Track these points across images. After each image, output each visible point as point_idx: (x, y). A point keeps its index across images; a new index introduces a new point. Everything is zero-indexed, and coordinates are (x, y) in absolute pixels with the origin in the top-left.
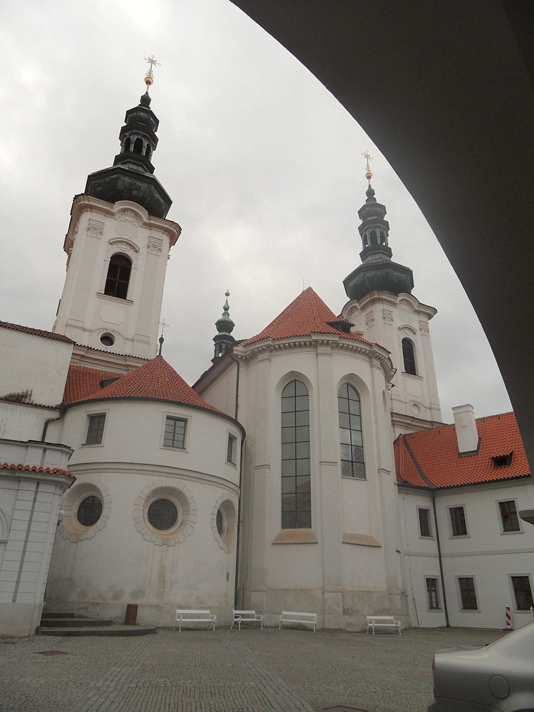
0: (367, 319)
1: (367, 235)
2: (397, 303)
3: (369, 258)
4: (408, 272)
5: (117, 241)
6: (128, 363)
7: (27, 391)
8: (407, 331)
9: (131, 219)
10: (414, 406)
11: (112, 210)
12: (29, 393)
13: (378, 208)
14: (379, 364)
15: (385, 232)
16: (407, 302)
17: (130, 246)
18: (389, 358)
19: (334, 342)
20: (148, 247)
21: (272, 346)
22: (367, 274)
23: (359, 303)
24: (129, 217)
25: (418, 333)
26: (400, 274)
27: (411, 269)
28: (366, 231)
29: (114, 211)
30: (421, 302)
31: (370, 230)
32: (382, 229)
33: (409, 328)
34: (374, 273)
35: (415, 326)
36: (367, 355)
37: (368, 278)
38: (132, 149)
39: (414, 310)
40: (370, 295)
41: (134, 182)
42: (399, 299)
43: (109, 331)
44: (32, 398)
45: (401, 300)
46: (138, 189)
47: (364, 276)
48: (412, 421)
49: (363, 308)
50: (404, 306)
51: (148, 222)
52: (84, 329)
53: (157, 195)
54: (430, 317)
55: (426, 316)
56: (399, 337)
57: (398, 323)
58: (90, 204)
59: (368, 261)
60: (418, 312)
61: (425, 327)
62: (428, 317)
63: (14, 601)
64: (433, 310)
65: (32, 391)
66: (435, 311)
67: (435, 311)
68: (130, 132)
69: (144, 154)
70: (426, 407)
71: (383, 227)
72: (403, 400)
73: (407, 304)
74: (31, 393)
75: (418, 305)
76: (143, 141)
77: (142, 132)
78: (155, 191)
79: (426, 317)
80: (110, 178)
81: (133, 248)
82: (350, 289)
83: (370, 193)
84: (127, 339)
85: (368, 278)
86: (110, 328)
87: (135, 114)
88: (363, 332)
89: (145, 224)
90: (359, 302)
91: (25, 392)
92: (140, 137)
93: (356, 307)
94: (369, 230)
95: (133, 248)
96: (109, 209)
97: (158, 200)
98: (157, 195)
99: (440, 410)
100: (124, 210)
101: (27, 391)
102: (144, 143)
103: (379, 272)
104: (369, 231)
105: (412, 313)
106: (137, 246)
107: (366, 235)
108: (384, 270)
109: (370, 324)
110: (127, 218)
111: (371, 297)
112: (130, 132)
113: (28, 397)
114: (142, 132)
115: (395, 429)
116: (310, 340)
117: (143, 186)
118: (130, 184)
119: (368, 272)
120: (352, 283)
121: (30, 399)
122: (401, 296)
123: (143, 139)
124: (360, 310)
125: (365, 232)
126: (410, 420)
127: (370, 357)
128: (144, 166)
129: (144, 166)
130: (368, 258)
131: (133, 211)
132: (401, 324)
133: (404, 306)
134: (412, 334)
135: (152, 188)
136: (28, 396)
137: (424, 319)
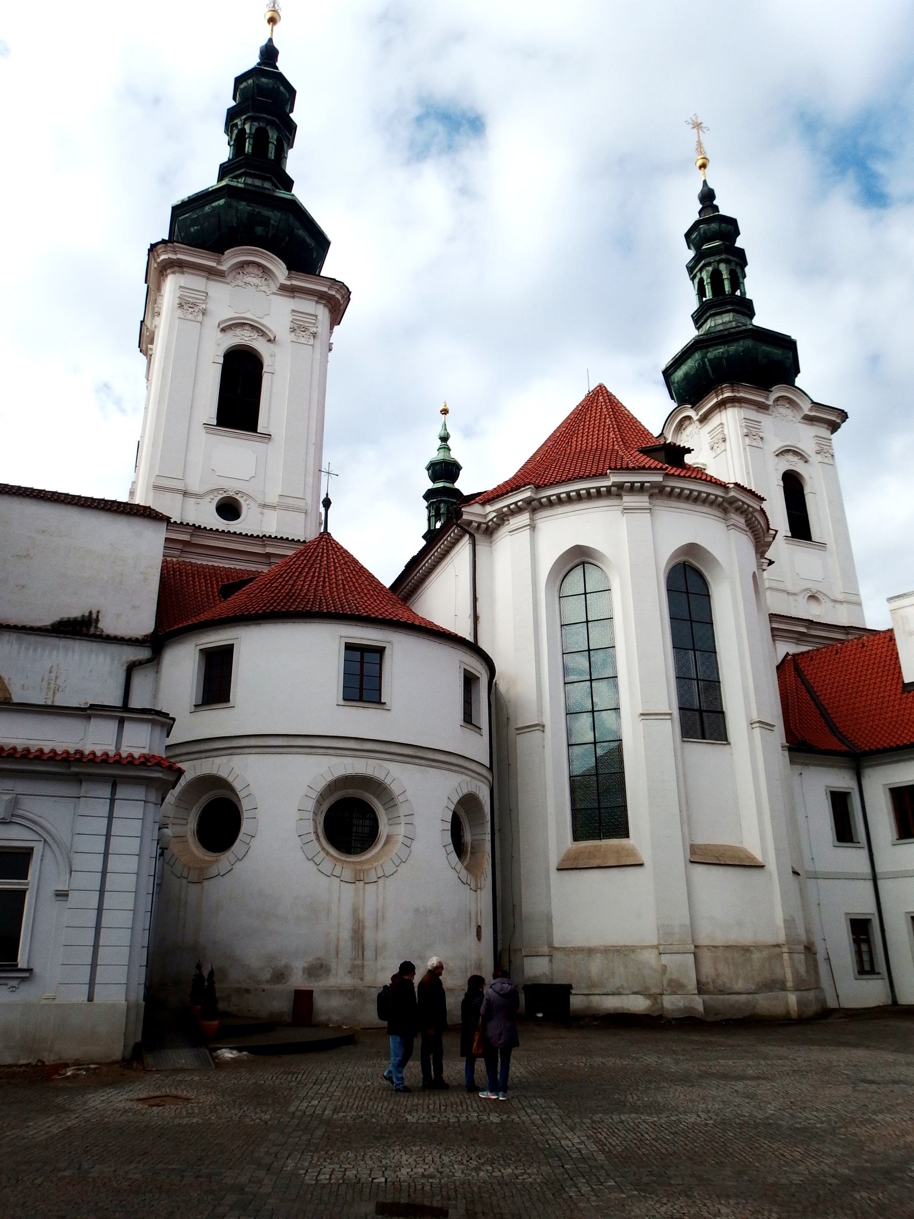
0: (712, 439)
1: (705, 278)
2: (770, 405)
3: (710, 324)
4: (788, 345)
5: (233, 325)
6: (269, 550)
7: (91, 613)
8: (790, 457)
9: (256, 281)
10: (811, 598)
12: (94, 616)
13: (723, 225)
14: (744, 522)
15: (738, 270)
16: (788, 401)
17: (258, 332)
18: (762, 509)
19: (654, 485)
20: (293, 330)
21: (534, 500)
22: (707, 352)
23: (695, 410)
24: (252, 278)
25: (814, 459)
26: (771, 350)
27: (792, 338)
28: (701, 270)
29: (224, 267)
30: (815, 401)
31: (710, 269)
32: (733, 264)
33: (794, 451)
34: (721, 350)
36: (720, 505)
37: (709, 360)
39: (802, 416)
40: (716, 392)
41: (257, 210)
42: (774, 396)
43: (231, 494)
44: (100, 625)
45: (777, 399)
46: (265, 222)
47: (703, 359)
48: (807, 628)
49: (703, 419)
50: (782, 410)
51: (288, 283)
52: (185, 494)
53: (301, 232)
54: (834, 427)
55: (826, 426)
56: (776, 470)
57: (775, 443)
59: (710, 327)
61: (825, 447)
62: (830, 428)
63: (90, 999)
64: (839, 414)
65: (98, 612)
66: (844, 415)
67: (844, 415)
68: (244, 117)
69: (272, 155)
70: (835, 601)
71: (734, 261)
72: (790, 589)
73: (787, 406)
74: (98, 616)
75: (810, 406)
76: (269, 131)
77: (265, 116)
78: (297, 224)
79: (827, 429)
82: (676, 385)
83: (707, 197)
85: (709, 360)
86: (231, 487)
87: (250, 81)
88: (705, 465)
89: (283, 288)
90: (695, 407)
91: (87, 614)
93: (689, 418)
94: (707, 268)
96: (214, 264)
97: (304, 240)
98: (301, 232)
99: (859, 604)
100: (242, 265)
101: (91, 613)
102: (270, 135)
104: (707, 271)
105: (799, 422)
106: (270, 330)
107: (701, 280)
108: (741, 342)
109: (719, 449)
110: (248, 279)
111: (717, 396)
112: (244, 117)
113: (93, 625)
114: (265, 116)
115: (777, 645)
116: (609, 483)
117: (274, 216)
118: (251, 215)
119: (711, 349)
120: (679, 374)
121: (96, 627)
122: (778, 392)
124: (697, 423)
125: (701, 273)
126: (803, 626)
127: (725, 511)
128: (273, 179)
129: (273, 179)
130: (709, 321)
131: (259, 265)
133: (784, 410)
134: (801, 463)
135: (291, 219)
136: (93, 621)
137: (824, 432)
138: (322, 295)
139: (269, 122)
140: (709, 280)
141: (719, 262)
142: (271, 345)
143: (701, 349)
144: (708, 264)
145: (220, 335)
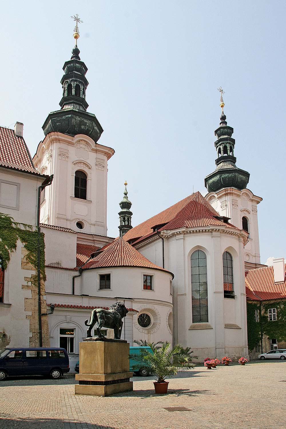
6: (95, 239)
9: (83, 146)
11: (73, 142)
20: (96, 165)
24: (82, 145)
25: (252, 212)
28: (220, 145)
29: (74, 142)
35: (250, 209)
38: (73, 93)
42: (242, 192)
43: (81, 220)
46: (85, 124)
50: (244, 197)
51: (95, 148)
57: (241, 207)
58: (59, 138)
60: (252, 200)
66: (262, 199)
67: (262, 199)
68: (71, 79)
75: (252, 196)
77: (79, 80)
80: (66, 117)
81: (88, 166)
84: (91, 224)
86: (81, 219)
87: (72, 64)
89: (93, 150)
92: (78, 83)
95: (88, 166)
96: (71, 141)
100: (79, 141)
103: (230, 175)
106: (90, 165)
107: (220, 149)
110: (81, 146)
112: (71, 79)
114: (79, 80)
117: (88, 122)
123: (80, 85)
130: (222, 163)
131: (85, 141)
132: (243, 208)
133: (244, 197)
137: (254, 204)
138: (106, 153)
139: (80, 82)
140: (223, 149)
141: (227, 143)
142: (90, 170)
143: (220, 174)
144: (223, 143)
145: (73, 165)
